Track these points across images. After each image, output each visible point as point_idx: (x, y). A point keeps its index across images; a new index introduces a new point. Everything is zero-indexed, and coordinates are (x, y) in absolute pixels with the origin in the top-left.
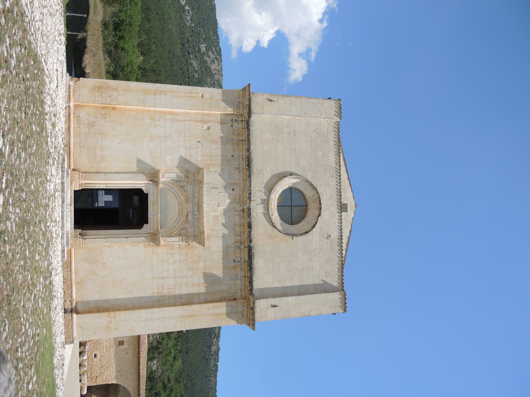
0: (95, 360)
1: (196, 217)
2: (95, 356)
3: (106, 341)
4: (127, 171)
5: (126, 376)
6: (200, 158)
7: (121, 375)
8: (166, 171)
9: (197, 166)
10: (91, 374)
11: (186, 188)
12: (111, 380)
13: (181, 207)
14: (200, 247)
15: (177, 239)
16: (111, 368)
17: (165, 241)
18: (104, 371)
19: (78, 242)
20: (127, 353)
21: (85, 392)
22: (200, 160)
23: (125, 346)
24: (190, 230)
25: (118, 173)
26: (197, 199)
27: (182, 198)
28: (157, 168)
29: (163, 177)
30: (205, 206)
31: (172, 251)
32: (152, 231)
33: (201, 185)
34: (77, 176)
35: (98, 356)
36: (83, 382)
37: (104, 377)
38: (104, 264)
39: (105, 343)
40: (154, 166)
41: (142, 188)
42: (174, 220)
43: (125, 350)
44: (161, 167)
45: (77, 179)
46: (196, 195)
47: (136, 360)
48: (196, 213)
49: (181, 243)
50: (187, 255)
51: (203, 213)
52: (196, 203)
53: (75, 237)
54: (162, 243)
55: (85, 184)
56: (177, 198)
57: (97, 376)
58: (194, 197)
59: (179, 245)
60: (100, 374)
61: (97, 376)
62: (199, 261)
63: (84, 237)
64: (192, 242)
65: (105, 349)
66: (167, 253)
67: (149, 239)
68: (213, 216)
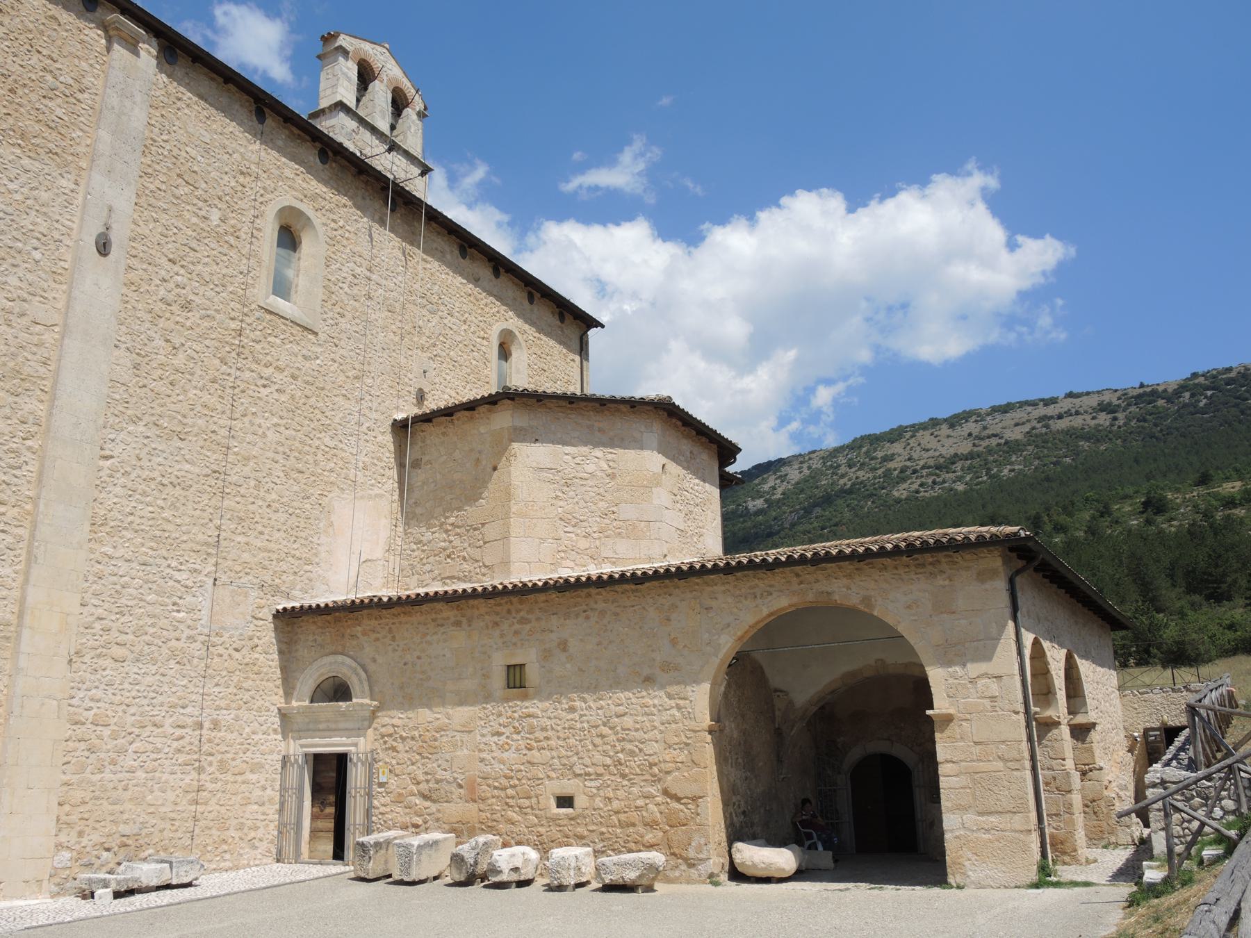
0: (580, 801)
2: (565, 801)
3: (501, 748)
5: (674, 642)
7: (667, 667)
10: (651, 825)
12: (689, 716)
16: (628, 721)
18: (639, 759)
20: (563, 645)
21: (783, 859)
23: (528, 656)
35: (568, 786)
36: (630, 875)
37: (668, 755)
39: (510, 755)
43: (546, 655)
47: (600, 600)
57: (666, 792)
60: (656, 780)
61: (666, 792)
65: (535, 755)
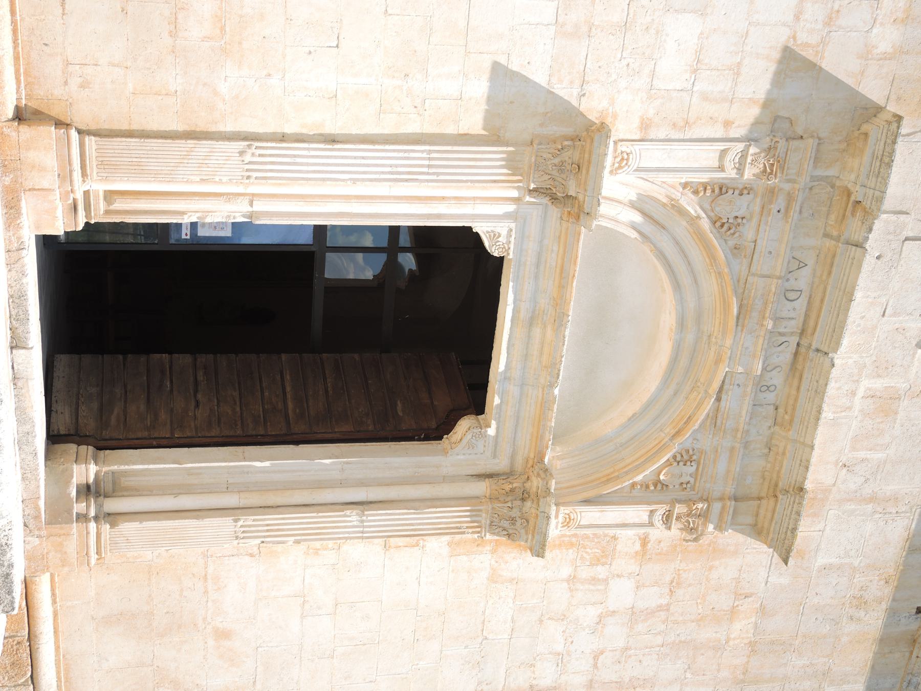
1: (770, 397)
4: (387, 127)
6: (886, 38)
8: (645, 125)
9: (854, 94)
11: (748, 232)
13: (690, 337)
14: (758, 554)
15: (637, 513)
17: (568, 522)
19: (72, 546)
22: (884, 47)
24: (722, 466)
25: (332, 140)
26: (801, 304)
27: (710, 285)
28: (593, 107)
29: (623, 161)
30: (845, 357)
31: (601, 571)
32: (501, 464)
33: (853, 228)
34: (50, 160)
38: (223, 635)
40: (567, 92)
41: (478, 228)
42: (636, 407)
44: (614, 98)
45: (49, 180)
46: (803, 279)
48: (777, 378)
49: (658, 532)
50: (674, 586)
51: (820, 392)
52: (794, 325)
53: (58, 514)
54: (554, 530)
55: (110, 196)
56: (677, 286)
58: (787, 295)
59: (644, 541)
62: (733, 613)
63: (112, 505)
64: (719, 527)
66: (572, 580)
67: (485, 519)
68: (871, 396)
